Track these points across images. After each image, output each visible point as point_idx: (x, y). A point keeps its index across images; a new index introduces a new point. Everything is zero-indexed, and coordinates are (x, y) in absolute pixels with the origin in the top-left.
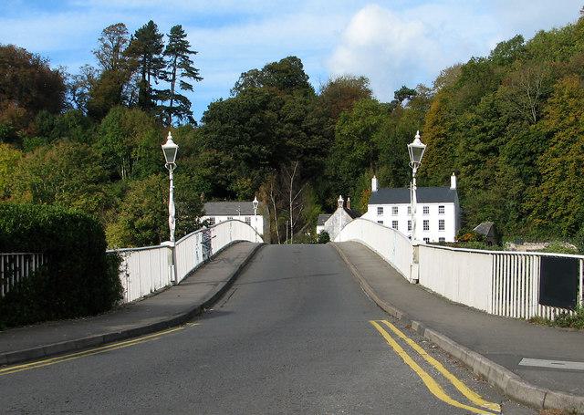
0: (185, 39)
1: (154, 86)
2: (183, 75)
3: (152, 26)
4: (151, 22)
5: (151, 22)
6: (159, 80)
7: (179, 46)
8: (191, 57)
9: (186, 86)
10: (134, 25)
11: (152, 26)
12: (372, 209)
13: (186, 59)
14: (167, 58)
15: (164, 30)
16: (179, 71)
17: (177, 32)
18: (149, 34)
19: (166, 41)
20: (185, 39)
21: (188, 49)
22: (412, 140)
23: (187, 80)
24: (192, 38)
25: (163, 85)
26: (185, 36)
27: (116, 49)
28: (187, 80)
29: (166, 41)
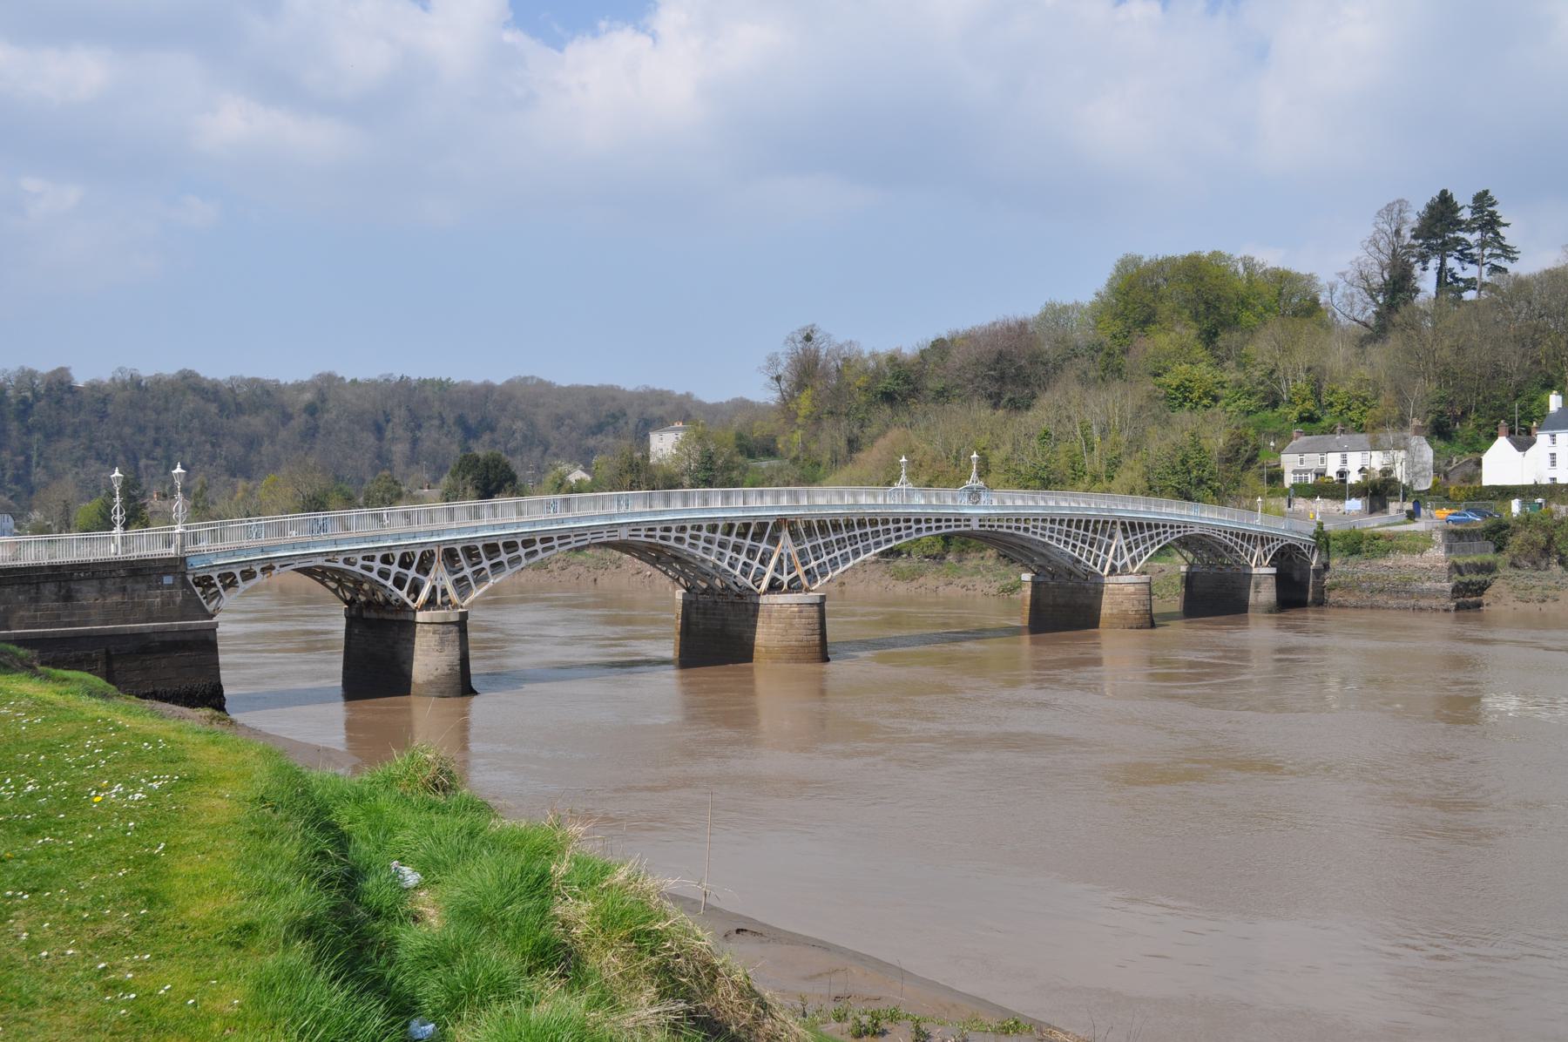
1: (1461, 275)
2: (1491, 255)
3: (1445, 200)
4: (1444, 192)
5: (1444, 192)
6: (1467, 265)
7: (1490, 224)
8: (1502, 230)
9: (1495, 269)
11: (1445, 200)
12: (1542, 438)
13: (1497, 234)
14: (1473, 238)
15: (1464, 200)
16: (1487, 252)
19: (1465, 215)
21: (1501, 220)
22: (175, 468)
25: (1471, 271)
27: (1397, 233)
28: (1495, 262)
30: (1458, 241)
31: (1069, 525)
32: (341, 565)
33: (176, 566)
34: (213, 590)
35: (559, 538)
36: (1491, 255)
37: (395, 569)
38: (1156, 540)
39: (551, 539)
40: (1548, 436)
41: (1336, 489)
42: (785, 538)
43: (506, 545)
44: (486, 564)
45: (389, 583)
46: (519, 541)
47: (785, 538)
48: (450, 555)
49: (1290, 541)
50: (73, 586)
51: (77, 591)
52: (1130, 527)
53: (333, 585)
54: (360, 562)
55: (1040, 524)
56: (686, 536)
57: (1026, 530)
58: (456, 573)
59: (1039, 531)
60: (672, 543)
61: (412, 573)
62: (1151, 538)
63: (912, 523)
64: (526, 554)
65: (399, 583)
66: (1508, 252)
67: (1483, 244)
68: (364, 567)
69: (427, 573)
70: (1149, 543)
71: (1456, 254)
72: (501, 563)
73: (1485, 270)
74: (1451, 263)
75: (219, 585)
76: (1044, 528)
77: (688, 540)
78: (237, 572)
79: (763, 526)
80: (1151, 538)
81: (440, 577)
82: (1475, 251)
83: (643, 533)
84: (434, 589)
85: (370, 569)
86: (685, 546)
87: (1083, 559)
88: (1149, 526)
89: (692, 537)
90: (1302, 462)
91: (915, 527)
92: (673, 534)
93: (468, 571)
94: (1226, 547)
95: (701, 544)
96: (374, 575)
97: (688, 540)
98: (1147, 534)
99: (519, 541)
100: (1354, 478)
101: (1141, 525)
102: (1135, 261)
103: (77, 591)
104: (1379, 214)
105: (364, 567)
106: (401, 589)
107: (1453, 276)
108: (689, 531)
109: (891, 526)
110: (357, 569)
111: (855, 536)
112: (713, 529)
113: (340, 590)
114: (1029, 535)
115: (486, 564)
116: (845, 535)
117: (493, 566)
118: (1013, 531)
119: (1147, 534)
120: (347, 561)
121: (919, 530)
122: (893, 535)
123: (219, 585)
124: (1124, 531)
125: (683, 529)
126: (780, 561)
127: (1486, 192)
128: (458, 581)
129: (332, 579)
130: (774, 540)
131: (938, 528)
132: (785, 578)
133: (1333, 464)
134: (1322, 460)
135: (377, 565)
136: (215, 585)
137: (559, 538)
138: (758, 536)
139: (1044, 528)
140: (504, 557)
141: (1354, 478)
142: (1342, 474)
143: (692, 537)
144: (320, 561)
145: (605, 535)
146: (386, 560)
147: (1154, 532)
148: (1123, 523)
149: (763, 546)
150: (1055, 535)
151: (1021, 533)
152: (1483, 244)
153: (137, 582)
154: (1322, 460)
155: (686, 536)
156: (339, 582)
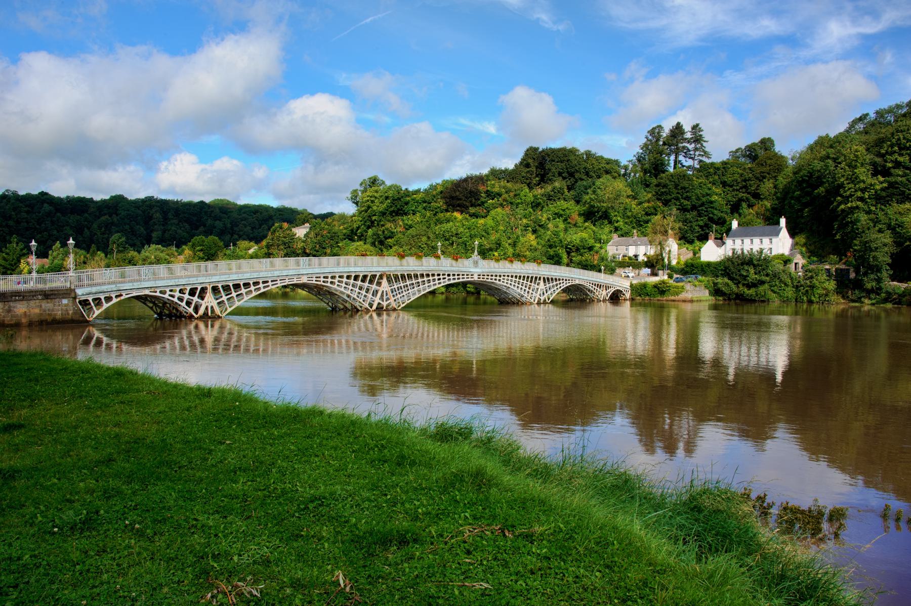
0: (701, 133)
1: (685, 164)
2: (700, 155)
4: (678, 124)
5: (678, 124)
6: (687, 159)
8: (704, 144)
10: (668, 126)
13: (702, 145)
15: (687, 128)
16: (697, 153)
17: (695, 127)
18: (678, 130)
19: (688, 135)
20: (701, 133)
21: (704, 139)
22: (69, 240)
23: (700, 158)
24: (706, 135)
26: (702, 131)
28: (700, 158)
29: (688, 135)
30: (684, 147)
31: (520, 278)
32: (158, 294)
33: (68, 293)
34: (88, 307)
35: (272, 281)
36: (700, 155)
37: (186, 296)
38: (559, 286)
39: (267, 282)
40: (759, 240)
41: (633, 263)
42: (384, 281)
43: (245, 285)
44: (234, 294)
45: (184, 304)
46: (251, 283)
47: (384, 281)
48: (215, 290)
49: (618, 288)
50: (12, 304)
51: (14, 307)
52: (547, 280)
53: (151, 305)
54: (168, 293)
55: (506, 278)
56: (336, 281)
57: (499, 280)
58: (217, 299)
59: (506, 281)
60: (329, 284)
61: (195, 299)
62: (557, 285)
63: (446, 276)
64: (255, 290)
65: (189, 303)
66: (706, 154)
67: (696, 149)
68: (170, 296)
69: (203, 299)
70: (555, 288)
71: (683, 154)
72: (241, 294)
73: (696, 162)
74: (681, 158)
75: (92, 304)
76: (508, 280)
77: (337, 283)
78: (102, 298)
79: (374, 276)
80: (557, 285)
81: (210, 300)
82: (692, 153)
83: (314, 279)
84: (207, 308)
85: (173, 296)
86: (335, 286)
87: (526, 295)
88: (559, 280)
89: (339, 281)
90: (617, 250)
91: (447, 278)
92: (330, 280)
93: (224, 298)
94: (589, 290)
95: (344, 285)
96: (176, 300)
97: (337, 283)
98: (555, 283)
99: (251, 283)
100: (641, 258)
101: (552, 279)
102: (536, 149)
103: (14, 307)
104: (648, 132)
105: (170, 296)
106: (190, 307)
107: (681, 164)
108: (337, 279)
109: (436, 277)
110: (166, 296)
111: (418, 283)
112: (356, 278)
113: (154, 308)
114: (501, 283)
115: (234, 294)
116: (414, 281)
117: (237, 296)
118: (493, 281)
119: (555, 283)
120: (161, 292)
121: (449, 280)
122: (437, 282)
123: (92, 304)
124: (544, 281)
125: (333, 277)
126: (382, 295)
127: (697, 125)
128: (219, 303)
129: (151, 302)
130: (379, 284)
131: (458, 279)
132: (385, 304)
133: (632, 251)
134: (627, 249)
135: (177, 294)
136: (90, 304)
137: (272, 281)
138: (371, 282)
139: (508, 280)
140: (243, 291)
141: (641, 258)
142: (636, 256)
143: (339, 281)
144: (147, 292)
145: (295, 280)
146: (181, 291)
147: (558, 282)
148: (544, 278)
149: (374, 287)
150: (513, 283)
151: (497, 282)
152: (696, 149)
153: (48, 303)
154: (627, 249)
155: (336, 281)
156: (154, 303)
